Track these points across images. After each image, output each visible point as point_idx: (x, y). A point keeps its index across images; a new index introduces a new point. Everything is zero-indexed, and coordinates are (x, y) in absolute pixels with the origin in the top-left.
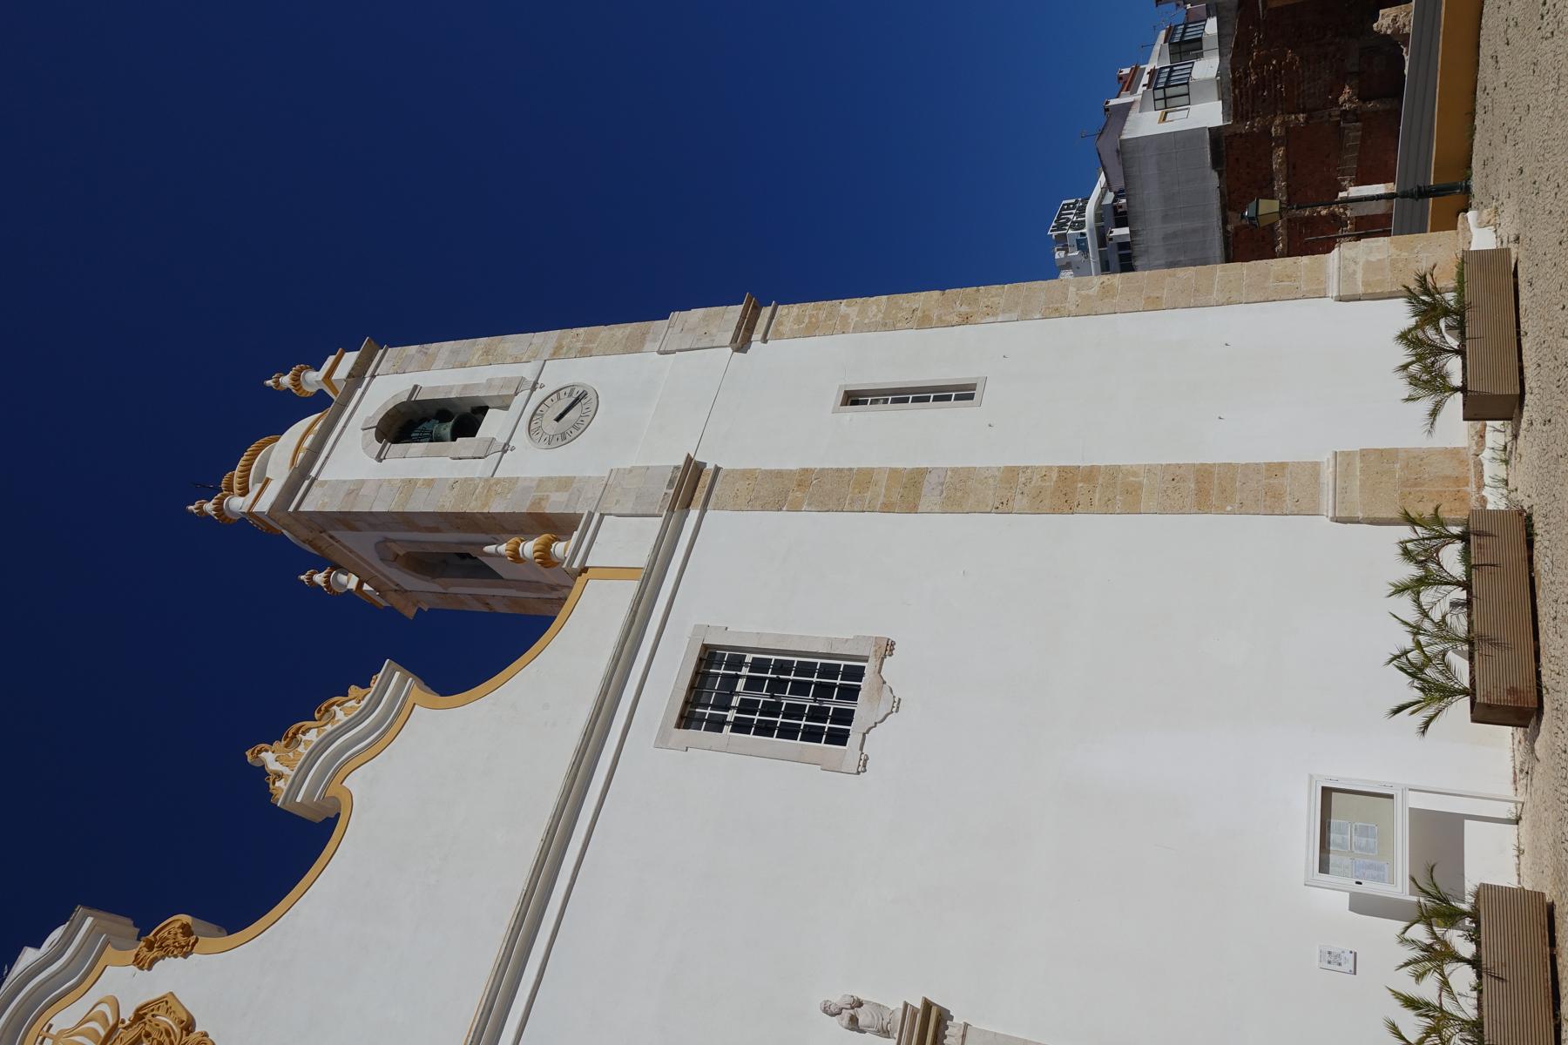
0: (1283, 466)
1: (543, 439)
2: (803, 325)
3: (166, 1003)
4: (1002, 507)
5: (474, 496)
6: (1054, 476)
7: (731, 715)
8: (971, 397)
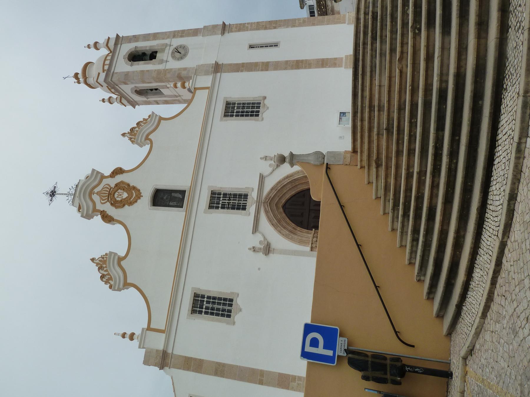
0: (337, 58)
1: (176, 59)
2: (238, 29)
3: (122, 182)
4: (286, 69)
5: (162, 74)
6: (295, 62)
7: (235, 114)
8: (277, 46)
